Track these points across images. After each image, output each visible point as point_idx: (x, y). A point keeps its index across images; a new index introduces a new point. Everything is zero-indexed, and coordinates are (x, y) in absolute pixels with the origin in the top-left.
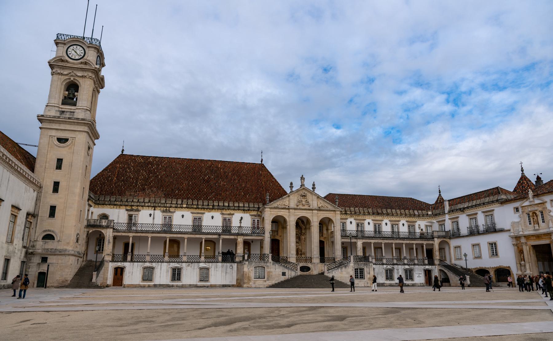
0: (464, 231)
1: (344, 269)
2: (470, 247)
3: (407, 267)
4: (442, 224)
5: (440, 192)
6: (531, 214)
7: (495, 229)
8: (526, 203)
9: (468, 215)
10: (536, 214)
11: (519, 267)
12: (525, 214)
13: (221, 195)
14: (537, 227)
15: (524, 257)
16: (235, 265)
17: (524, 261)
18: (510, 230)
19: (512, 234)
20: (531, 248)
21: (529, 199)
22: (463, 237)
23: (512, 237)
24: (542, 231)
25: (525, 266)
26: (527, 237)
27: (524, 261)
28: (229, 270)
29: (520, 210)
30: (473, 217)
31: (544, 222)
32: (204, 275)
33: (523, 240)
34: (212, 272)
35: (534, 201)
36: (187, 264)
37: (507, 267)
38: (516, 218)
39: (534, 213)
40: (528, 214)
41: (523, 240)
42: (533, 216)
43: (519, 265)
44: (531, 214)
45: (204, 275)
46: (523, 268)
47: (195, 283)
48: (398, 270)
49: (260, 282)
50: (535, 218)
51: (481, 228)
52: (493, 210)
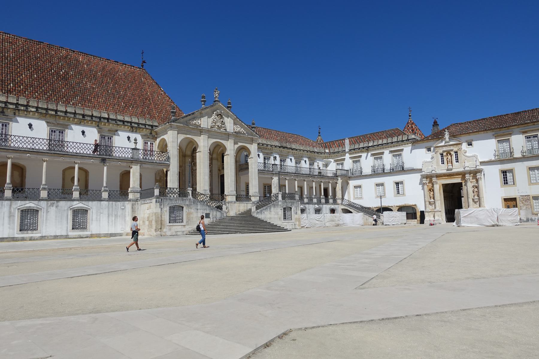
0: (367, 170)
1: (272, 209)
2: (373, 186)
3: (317, 206)
4: (341, 162)
5: (319, 133)
8: (443, 144)
9: (373, 155)
10: (450, 154)
13: (90, 101)
14: (450, 167)
16: (128, 205)
21: (445, 139)
22: (366, 176)
26: (439, 176)
27: (434, 198)
28: (120, 212)
30: (378, 156)
31: (457, 161)
32: (79, 219)
34: (92, 215)
36: (50, 202)
40: (442, 155)
44: (445, 154)
45: (79, 219)
47: (64, 233)
48: (309, 209)
49: (177, 228)
50: (449, 157)
51: (388, 168)
52: (402, 150)
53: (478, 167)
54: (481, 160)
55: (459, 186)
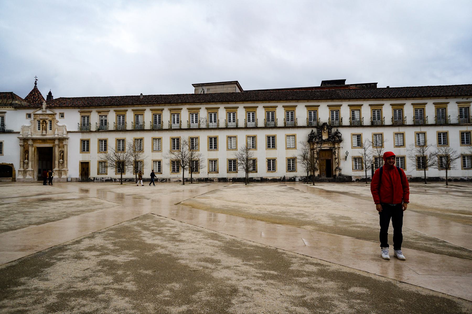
6: (41, 121)
7: (4, 130)
8: (40, 112)
10: (46, 122)
11: (22, 165)
12: (36, 121)
14: (44, 133)
15: (28, 156)
17: (28, 160)
18: (19, 133)
19: (21, 136)
20: (36, 149)
21: (42, 108)
23: (21, 139)
24: (48, 136)
25: (28, 163)
26: (34, 140)
29: (32, 116)
31: (51, 129)
33: (30, 142)
35: (46, 112)
37: (10, 164)
38: (27, 122)
39: (44, 121)
40: (39, 121)
41: (30, 142)
42: (43, 123)
43: (22, 163)
44: (41, 121)
46: (25, 165)
50: (44, 125)
52: (5, 113)
53: (65, 136)
54: (68, 130)
55: (50, 150)
